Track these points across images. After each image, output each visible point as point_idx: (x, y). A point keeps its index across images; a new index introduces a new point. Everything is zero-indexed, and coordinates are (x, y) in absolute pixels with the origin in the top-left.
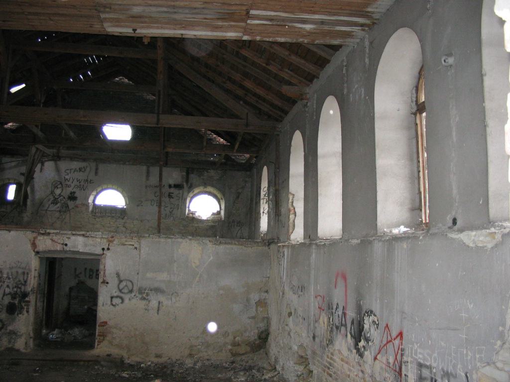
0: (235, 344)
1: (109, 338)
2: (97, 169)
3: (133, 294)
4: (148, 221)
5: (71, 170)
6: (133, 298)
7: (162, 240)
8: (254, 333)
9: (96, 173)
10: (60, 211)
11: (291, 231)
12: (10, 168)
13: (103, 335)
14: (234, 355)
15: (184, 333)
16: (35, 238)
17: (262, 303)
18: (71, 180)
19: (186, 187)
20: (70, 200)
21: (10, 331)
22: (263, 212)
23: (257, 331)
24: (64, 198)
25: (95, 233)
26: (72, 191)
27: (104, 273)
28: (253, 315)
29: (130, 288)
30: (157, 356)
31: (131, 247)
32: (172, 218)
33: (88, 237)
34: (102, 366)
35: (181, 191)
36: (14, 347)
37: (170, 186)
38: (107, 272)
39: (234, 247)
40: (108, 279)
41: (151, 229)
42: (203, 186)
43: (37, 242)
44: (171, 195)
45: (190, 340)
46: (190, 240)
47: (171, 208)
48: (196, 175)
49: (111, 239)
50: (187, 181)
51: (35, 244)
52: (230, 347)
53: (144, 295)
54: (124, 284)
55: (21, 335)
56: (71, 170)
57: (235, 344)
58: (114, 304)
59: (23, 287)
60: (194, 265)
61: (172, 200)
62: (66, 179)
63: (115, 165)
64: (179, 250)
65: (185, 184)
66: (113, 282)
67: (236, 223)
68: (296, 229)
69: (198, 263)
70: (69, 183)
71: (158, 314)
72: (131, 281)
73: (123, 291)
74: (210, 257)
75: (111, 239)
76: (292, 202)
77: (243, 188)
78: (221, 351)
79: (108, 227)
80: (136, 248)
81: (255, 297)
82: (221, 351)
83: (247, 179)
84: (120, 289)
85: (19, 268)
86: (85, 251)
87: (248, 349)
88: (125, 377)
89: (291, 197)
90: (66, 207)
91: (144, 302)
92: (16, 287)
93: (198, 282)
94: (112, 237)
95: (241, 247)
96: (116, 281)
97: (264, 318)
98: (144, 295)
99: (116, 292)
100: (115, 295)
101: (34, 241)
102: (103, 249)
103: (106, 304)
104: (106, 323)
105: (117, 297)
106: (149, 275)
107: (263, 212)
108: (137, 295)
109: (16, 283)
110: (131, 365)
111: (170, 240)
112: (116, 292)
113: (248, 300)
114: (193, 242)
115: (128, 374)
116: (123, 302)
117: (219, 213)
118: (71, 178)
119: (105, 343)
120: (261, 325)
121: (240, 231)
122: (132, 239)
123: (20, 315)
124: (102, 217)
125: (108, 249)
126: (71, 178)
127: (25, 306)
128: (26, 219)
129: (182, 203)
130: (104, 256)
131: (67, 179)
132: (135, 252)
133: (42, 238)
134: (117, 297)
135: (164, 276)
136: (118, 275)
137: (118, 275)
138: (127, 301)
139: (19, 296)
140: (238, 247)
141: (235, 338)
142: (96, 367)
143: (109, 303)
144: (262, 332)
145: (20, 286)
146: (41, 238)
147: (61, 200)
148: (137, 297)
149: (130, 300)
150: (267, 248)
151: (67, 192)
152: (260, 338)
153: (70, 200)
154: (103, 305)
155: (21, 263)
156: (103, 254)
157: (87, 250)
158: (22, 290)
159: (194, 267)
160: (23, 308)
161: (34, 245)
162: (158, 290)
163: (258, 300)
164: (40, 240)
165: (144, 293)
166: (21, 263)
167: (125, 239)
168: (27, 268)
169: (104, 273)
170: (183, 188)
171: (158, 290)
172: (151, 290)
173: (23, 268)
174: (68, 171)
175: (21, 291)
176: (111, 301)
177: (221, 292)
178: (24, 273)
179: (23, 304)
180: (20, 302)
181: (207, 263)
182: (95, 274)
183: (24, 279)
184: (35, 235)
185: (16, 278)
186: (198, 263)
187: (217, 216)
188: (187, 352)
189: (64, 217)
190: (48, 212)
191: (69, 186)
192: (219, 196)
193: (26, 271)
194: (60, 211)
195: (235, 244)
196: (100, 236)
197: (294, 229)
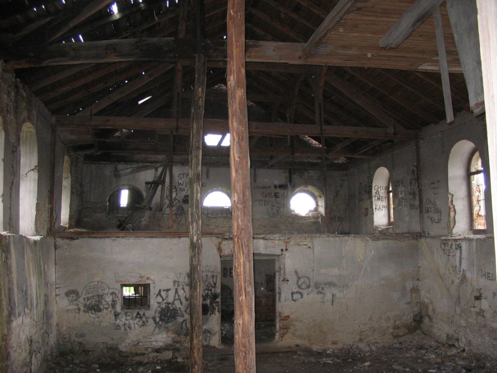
0: (396, 328)
1: (291, 330)
2: (208, 173)
3: (310, 289)
4: (258, 220)
5: (184, 174)
6: (310, 293)
7: (332, 239)
8: (410, 316)
9: (208, 177)
10: (176, 214)
11: (452, 226)
12: (126, 175)
13: (286, 328)
14: (395, 337)
15: (355, 320)
16: (220, 243)
17: (415, 290)
18: (185, 184)
19: (288, 187)
20: (185, 204)
21: (205, 330)
22: (376, 209)
23: (412, 314)
24: (179, 201)
25: (274, 236)
26: (186, 194)
27: (284, 272)
28: (409, 301)
29: (308, 283)
30: (334, 343)
31: (305, 246)
32: (279, 217)
33: (267, 239)
34: (299, 355)
35: (285, 192)
36: (210, 344)
37: (275, 187)
38: (287, 271)
39: (390, 241)
40: (288, 277)
41: (260, 227)
42: (304, 185)
43: (222, 247)
44: (277, 194)
45: (360, 326)
46: (354, 237)
47: (278, 207)
48: (296, 175)
49: (287, 240)
50: (290, 181)
51: (220, 248)
52: (391, 330)
53: (320, 289)
54: (302, 280)
55: (215, 333)
56: (184, 174)
57: (396, 328)
58: (295, 299)
59: (213, 289)
60: (359, 260)
61: (277, 199)
62: (180, 184)
63: (224, 169)
64: (347, 247)
65: (289, 184)
66: (293, 279)
67: (337, 219)
68: (456, 224)
69: (362, 258)
70: (182, 187)
71: (332, 305)
72: (308, 278)
73: (302, 287)
74: (371, 252)
75: (287, 240)
76: (452, 201)
77: (341, 186)
78: (385, 334)
79: (222, 227)
80: (309, 247)
81: (409, 285)
82: (385, 334)
83: (344, 178)
84: (299, 285)
85: (209, 271)
86: (267, 253)
87: (406, 331)
88: (330, 363)
89: (450, 197)
90: (181, 210)
91: (320, 296)
92: (206, 290)
93: (363, 274)
94: (289, 239)
95: (396, 241)
96: (295, 278)
97: (417, 302)
98: (320, 289)
99: (295, 289)
100: (295, 291)
101: (219, 246)
102: (282, 250)
103: (288, 300)
104: (288, 317)
105: (297, 292)
106: (322, 271)
107: (376, 209)
108: (314, 290)
109: (207, 286)
110: (319, 353)
111: (337, 239)
112: (295, 289)
113: (404, 288)
114: (357, 239)
115: (331, 360)
116: (302, 297)
117: (316, 209)
118: (185, 183)
119: (289, 335)
120: (416, 309)
121: (341, 226)
122: (306, 239)
123: (213, 315)
124: (215, 218)
125: (286, 250)
126: (185, 183)
127: (216, 306)
128: (144, 223)
129: (285, 204)
130: (283, 256)
131: (180, 183)
132: (309, 251)
133: (226, 243)
134: (297, 292)
135: (335, 271)
136: (296, 273)
137: (296, 273)
138: (305, 296)
139: (210, 298)
140: (394, 241)
141: (395, 322)
142: (294, 357)
143: (290, 298)
144: (416, 316)
145: (210, 288)
146: (225, 242)
147: (176, 204)
148: (314, 291)
149: (308, 294)
150: (416, 241)
151: (182, 195)
152: (414, 320)
153: (185, 204)
154: (285, 301)
155: (210, 267)
156: (282, 254)
157: (268, 252)
158: (213, 292)
159: (359, 261)
160: (215, 309)
161: (220, 249)
162: (331, 284)
163: (412, 287)
164: (225, 245)
165: (320, 287)
166: (210, 267)
167: (299, 240)
168: (216, 271)
169: (284, 272)
170: (288, 187)
171: (331, 284)
172: (325, 285)
173: (212, 272)
174: (181, 176)
175: (212, 293)
176: (292, 296)
177: (383, 282)
178: (213, 276)
179: (214, 305)
180: (211, 303)
181: (369, 258)
182: (228, 273)
183: (213, 282)
184: (219, 240)
185: (206, 281)
186: (362, 258)
187: (315, 213)
188: (358, 337)
189: (180, 220)
190: (165, 215)
191: (183, 190)
192: (317, 193)
193: (215, 274)
194: (176, 214)
195: (391, 239)
196: (279, 238)
197: (455, 224)
